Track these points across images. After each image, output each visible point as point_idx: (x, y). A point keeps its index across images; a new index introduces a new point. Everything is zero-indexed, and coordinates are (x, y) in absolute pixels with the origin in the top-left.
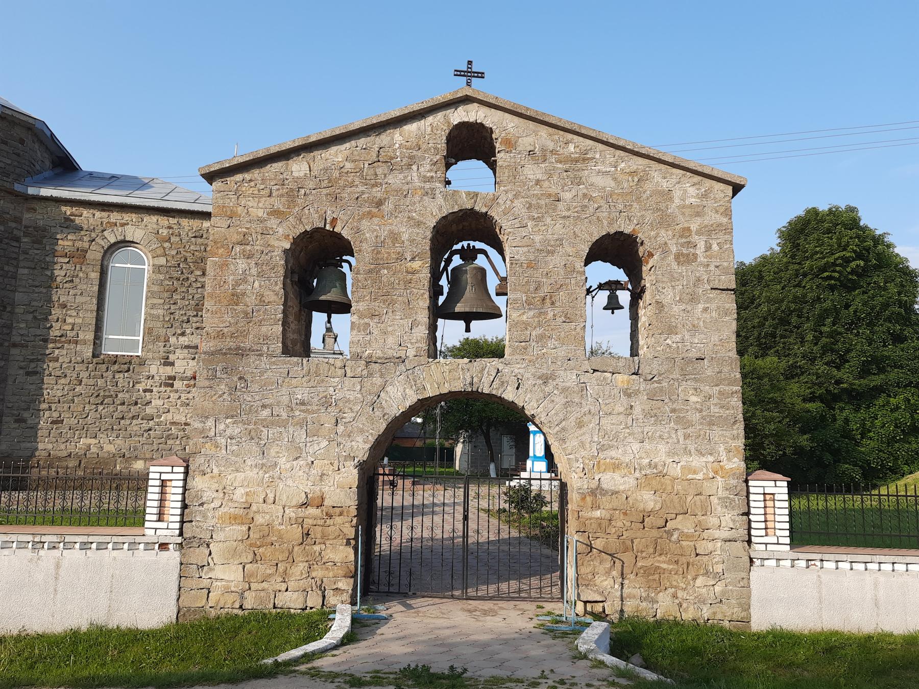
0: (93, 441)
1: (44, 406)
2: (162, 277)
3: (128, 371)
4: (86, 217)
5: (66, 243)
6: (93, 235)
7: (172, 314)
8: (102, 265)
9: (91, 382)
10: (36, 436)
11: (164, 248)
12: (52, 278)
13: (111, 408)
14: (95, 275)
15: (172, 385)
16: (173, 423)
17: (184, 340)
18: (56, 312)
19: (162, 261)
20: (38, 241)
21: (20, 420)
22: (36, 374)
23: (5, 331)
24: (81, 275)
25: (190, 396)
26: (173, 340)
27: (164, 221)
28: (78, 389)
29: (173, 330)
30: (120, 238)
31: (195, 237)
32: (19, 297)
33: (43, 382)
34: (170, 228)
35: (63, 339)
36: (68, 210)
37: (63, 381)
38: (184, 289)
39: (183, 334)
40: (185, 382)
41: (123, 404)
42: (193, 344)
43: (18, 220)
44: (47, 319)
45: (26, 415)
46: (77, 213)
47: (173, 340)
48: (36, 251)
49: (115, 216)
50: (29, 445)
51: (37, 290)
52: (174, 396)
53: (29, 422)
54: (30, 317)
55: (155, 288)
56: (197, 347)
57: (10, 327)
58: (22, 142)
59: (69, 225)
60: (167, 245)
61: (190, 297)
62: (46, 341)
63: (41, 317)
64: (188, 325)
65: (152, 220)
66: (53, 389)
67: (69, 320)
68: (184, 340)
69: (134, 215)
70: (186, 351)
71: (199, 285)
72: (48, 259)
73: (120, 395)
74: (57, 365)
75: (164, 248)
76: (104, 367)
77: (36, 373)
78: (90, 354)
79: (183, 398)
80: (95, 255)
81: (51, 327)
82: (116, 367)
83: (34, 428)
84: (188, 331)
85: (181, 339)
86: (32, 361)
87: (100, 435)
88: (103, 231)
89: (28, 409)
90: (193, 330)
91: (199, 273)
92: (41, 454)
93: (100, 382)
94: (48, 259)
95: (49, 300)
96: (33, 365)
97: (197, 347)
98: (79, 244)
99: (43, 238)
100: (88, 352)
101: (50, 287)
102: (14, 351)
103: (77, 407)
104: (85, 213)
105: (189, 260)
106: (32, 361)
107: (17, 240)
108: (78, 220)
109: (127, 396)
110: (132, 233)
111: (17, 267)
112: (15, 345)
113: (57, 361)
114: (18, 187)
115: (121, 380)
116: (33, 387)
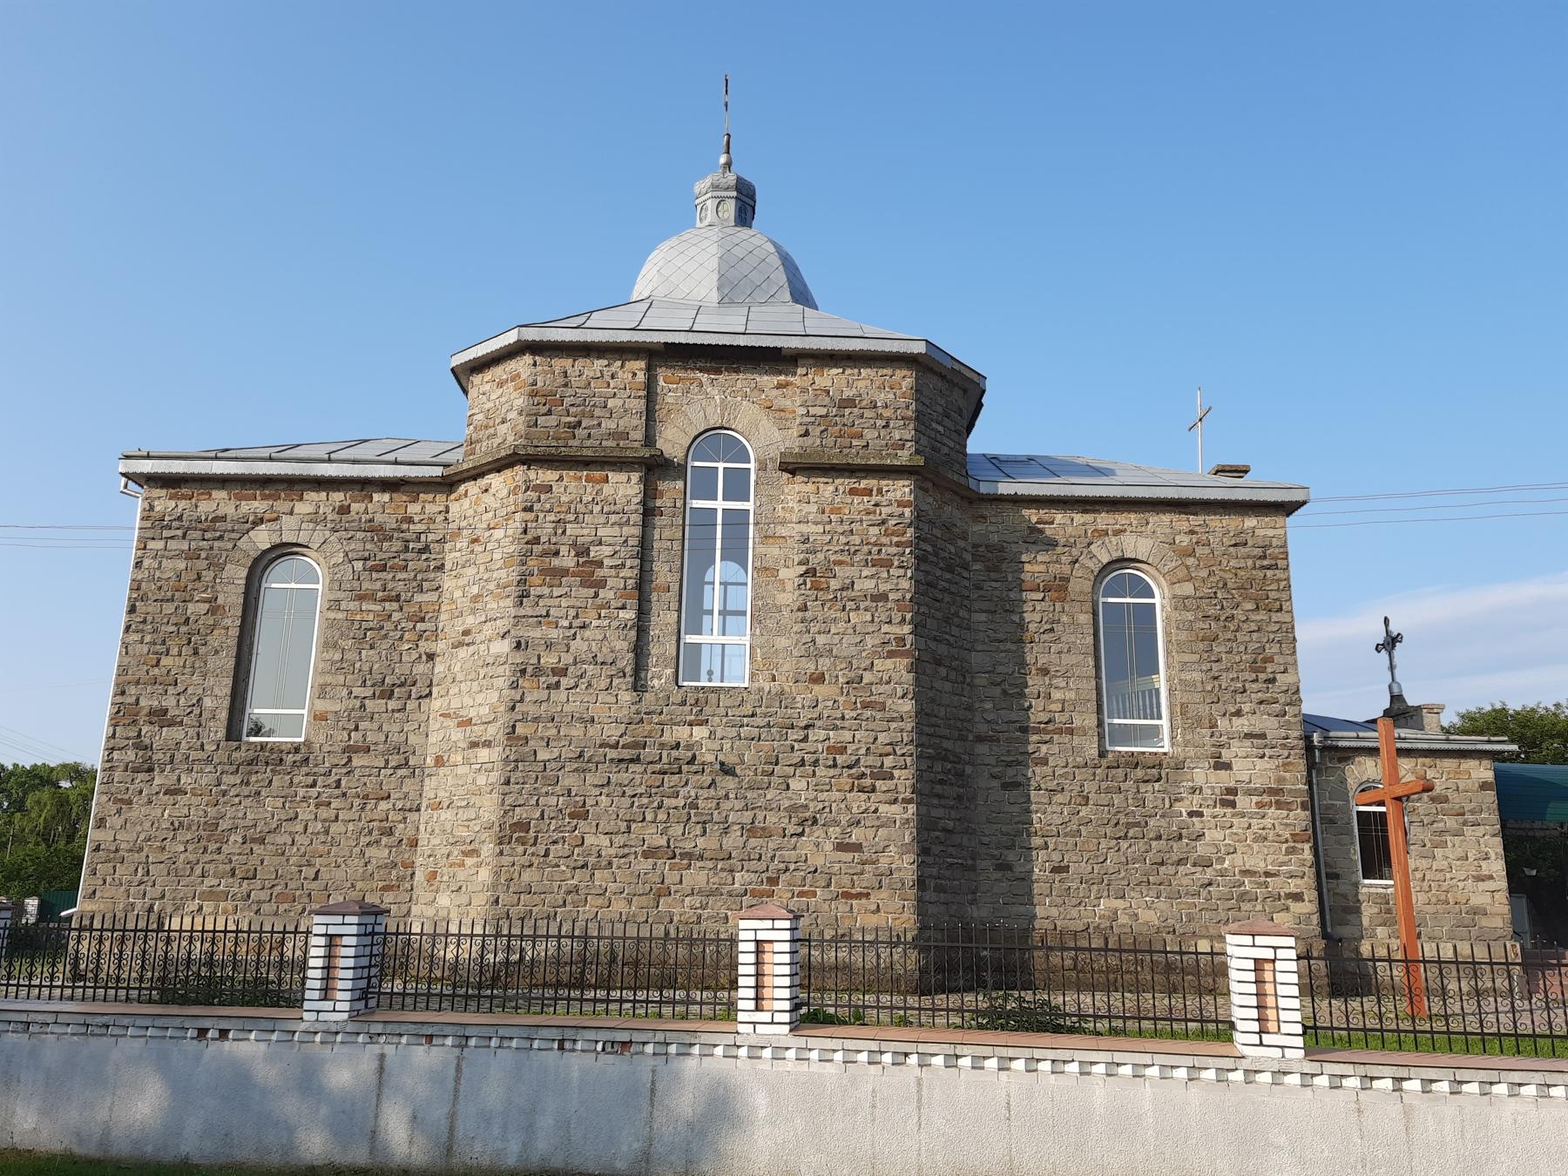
0: (1120, 904)
2: (1190, 616)
3: (1158, 780)
4: (1061, 523)
5: (1036, 567)
6: (1075, 552)
7: (1215, 678)
10: (1030, 894)
11: (1188, 568)
12: (1022, 626)
15: (1233, 804)
16: (1245, 873)
17: (1243, 725)
18: (1034, 683)
19: (1187, 589)
21: (1005, 867)
22: (1018, 785)
24: (1064, 619)
25: (1268, 822)
26: (1222, 724)
27: (1183, 522)
28: (1084, 812)
30: (1116, 555)
31: (1235, 545)
33: (1029, 801)
34: (1192, 532)
35: (1050, 727)
36: (1032, 515)
37: (1059, 798)
38: (1229, 635)
39: (1238, 713)
40: (1255, 799)
41: (1159, 838)
42: (1257, 730)
44: (1022, 695)
45: (1011, 856)
46: (1046, 518)
48: (995, 584)
49: (1104, 520)
50: (1022, 909)
51: (1002, 646)
53: (1017, 869)
54: (997, 691)
56: (1263, 736)
59: (1036, 538)
60: (1191, 561)
61: (1242, 648)
62: (1025, 730)
63: (1014, 692)
64: (1244, 698)
66: (1046, 814)
67: (1056, 695)
68: (1243, 725)
69: (1133, 516)
70: (1248, 743)
71: (1253, 627)
72: (1012, 595)
73: (1152, 822)
74: (1047, 770)
75: (1188, 568)
77: (1017, 785)
78: (1095, 752)
79: (1255, 828)
81: (1030, 707)
82: (1139, 773)
83: (1026, 879)
84: (1246, 708)
86: (1009, 765)
87: (1130, 894)
88: (1089, 544)
89: (1011, 847)
90: (1253, 706)
91: (1250, 606)
93: (1117, 799)
94: (1012, 595)
95: (1023, 664)
96: (1011, 772)
101: (1021, 641)
102: (982, 749)
104: (1059, 517)
105: (1230, 585)
106: (1009, 765)
108: (1049, 531)
109: (1163, 823)
112: (980, 739)
113: (1046, 764)
115: (1149, 796)
116: (1015, 809)
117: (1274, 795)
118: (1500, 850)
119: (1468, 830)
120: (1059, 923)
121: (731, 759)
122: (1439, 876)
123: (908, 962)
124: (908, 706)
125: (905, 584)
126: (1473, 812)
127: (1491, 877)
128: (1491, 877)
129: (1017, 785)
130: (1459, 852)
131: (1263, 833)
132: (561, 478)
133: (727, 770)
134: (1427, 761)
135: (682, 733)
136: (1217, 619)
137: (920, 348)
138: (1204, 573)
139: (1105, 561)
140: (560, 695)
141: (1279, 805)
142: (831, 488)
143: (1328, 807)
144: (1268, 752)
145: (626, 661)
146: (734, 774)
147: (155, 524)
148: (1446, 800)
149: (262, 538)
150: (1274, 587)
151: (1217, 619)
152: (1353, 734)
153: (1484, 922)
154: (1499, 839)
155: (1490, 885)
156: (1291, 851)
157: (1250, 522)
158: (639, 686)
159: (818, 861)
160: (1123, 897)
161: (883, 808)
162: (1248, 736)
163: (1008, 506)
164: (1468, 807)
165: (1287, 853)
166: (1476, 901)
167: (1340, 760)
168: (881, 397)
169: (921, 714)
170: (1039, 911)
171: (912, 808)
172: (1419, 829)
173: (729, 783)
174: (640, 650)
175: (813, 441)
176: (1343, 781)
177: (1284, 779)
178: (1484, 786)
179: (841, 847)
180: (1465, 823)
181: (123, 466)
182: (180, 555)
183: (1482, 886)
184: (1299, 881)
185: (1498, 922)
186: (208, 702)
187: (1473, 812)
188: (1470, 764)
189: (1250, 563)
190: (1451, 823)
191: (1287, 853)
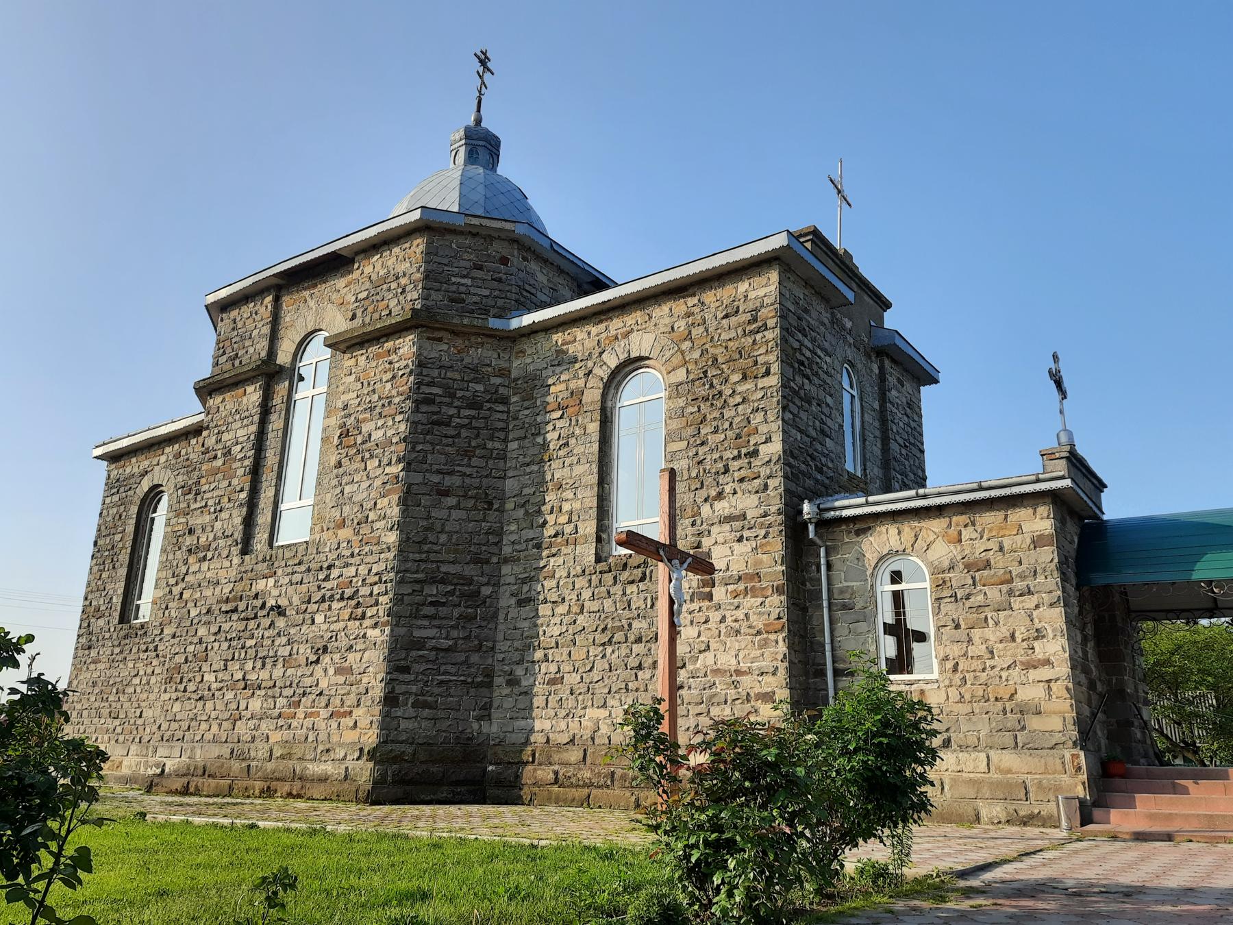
0: (603, 713)
1: (539, 655)
2: (681, 402)
3: (643, 579)
4: (581, 340)
6: (590, 364)
7: (700, 463)
8: (603, 409)
9: (595, 606)
10: (531, 707)
11: (683, 353)
12: (545, 446)
13: (624, 651)
14: (594, 427)
15: (710, 597)
16: (716, 672)
17: (723, 507)
18: (551, 497)
19: (681, 375)
20: (528, 397)
21: (513, 682)
22: (527, 601)
23: (492, 539)
24: (578, 431)
25: (740, 614)
26: (706, 510)
27: (679, 306)
28: (580, 618)
29: (703, 494)
30: (623, 357)
31: (726, 316)
32: (510, 485)
33: (537, 616)
34: (688, 315)
35: (559, 539)
36: (558, 337)
37: (561, 609)
38: (716, 414)
39: (720, 496)
40: (731, 588)
41: (639, 640)
42: (737, 513)
43: (504, 373)
44: (539, 512)
45: (519, 671)
46: (568, 338)
47: (706, 510)
48: (526, 412)
49: (616, 325)
50: (522, 723)
51: (528, 470)
52: (715, 616)
53: (524, 683)
54: (521, 512)
55: (675, 424)
57: (500, 533)
58: (504, 261)
59: (562, 360)
60: (686, 345)
61: (727, 425)
62: (539, 546)
63: (533, 512)
64: (728, 478)
65: (661, 312)
66: (551, 624)
67: (566, 507)
68: (723, 507)
69: (639, 313)
70: (726, 527)
71: (738, 399)
72: (539, 419)
73: (636, 624)
74: (553, 583)
75: (683, 353)
76: (608, 578)
77: (529, 600)
78: (592, 558)
79: (729, 619)
80: (593, 396)
81: (545, 523)
82: (625, 576)
83: (528, 693)
84: (728, 489)
85: (719, 505)
86: (524, 581)
87: (611, 702)
88: (601, 354)
89: (520, 662)
90: (736, 485)
91: (736, 377)
92: (538, 738)
93: (608, 604)
94: (539, 419)
95: (543, 482)
96: (525, 588)
97: (744, 516)
98: (573, 385)
99: (533, 386)
100: (588, 552)
101: (542, 461)
102: (506, 569)
103: (579, 654)
104: (579, 333)
105: (720, 360)
106: (524, 581)
107: (505, 401)
108: (571, 349)
109: (644, 625)
110: (641, 344)
111: (505, 441)
112: (506, 561)
113: (553, 577)
114: (494, 323)
115: (634, 597)
116: (526, 624)
117: (749, 581)
118: (1061, 623)
119: (1016, 602)
120: (551, 736)
121: (283, 602)
122: (976, 664)
123: (364, 771)
124: (392, 538)
125: (402, 427)
126: (1022, 577)
127: (1047, 662)
128: (1047, 662)
129: (529, 600)
130: (1004, 631)
131: (736, 625)
132: (224, 400)
133: (280, 611)
134: (963, 519)
135: (261, 585)
136: (705, 399)
137: (416, 215)
138: (696, 355)
139: (613, 366)
140: (205, 566)
141: (753, 592)
142: (364, 357)
143: (842, 591)
144: (746, 534)
145: (238, 535)
146: (285, 615)
147: (113, 486)
148: (988, 565)
149: (146, 485)
150: (762, 350)
151: (705, 399)
152: (862, 500)
153: (1034, 723)
154: (1059, 611)
155: (1045, 673)
156: (764, 644)
157: (743, 287)
158: (246, 550)
159: (323, 684)
160: (604, 706)
161: (370, 632)
162: (729, 519)
163: (542, 335)
164: (1016, 570)
165: (760, 647)
166: (1025, 694)
167: (858, 533)
168: (402, 267)
169: (404, 546)
170: (538, 725)
171: (387, 630)
172: (952, 606)
173: (281, 623)
174: (249, 523)
175: (358, 322)
176: (861, 557)
177: (761, 562)
178: (1037, 542)
179: (338, 671)
180: (1011, 593)
181: (99, 451)
182: (115, 505)
183: (1034, 674)
184: (769, 679)
185: (1055, 723)
186: (114, 600)
187: (1022, 577)
188: (1021, 515)
189: (740, 330)
190: (994, 594)
191: (760, 647)
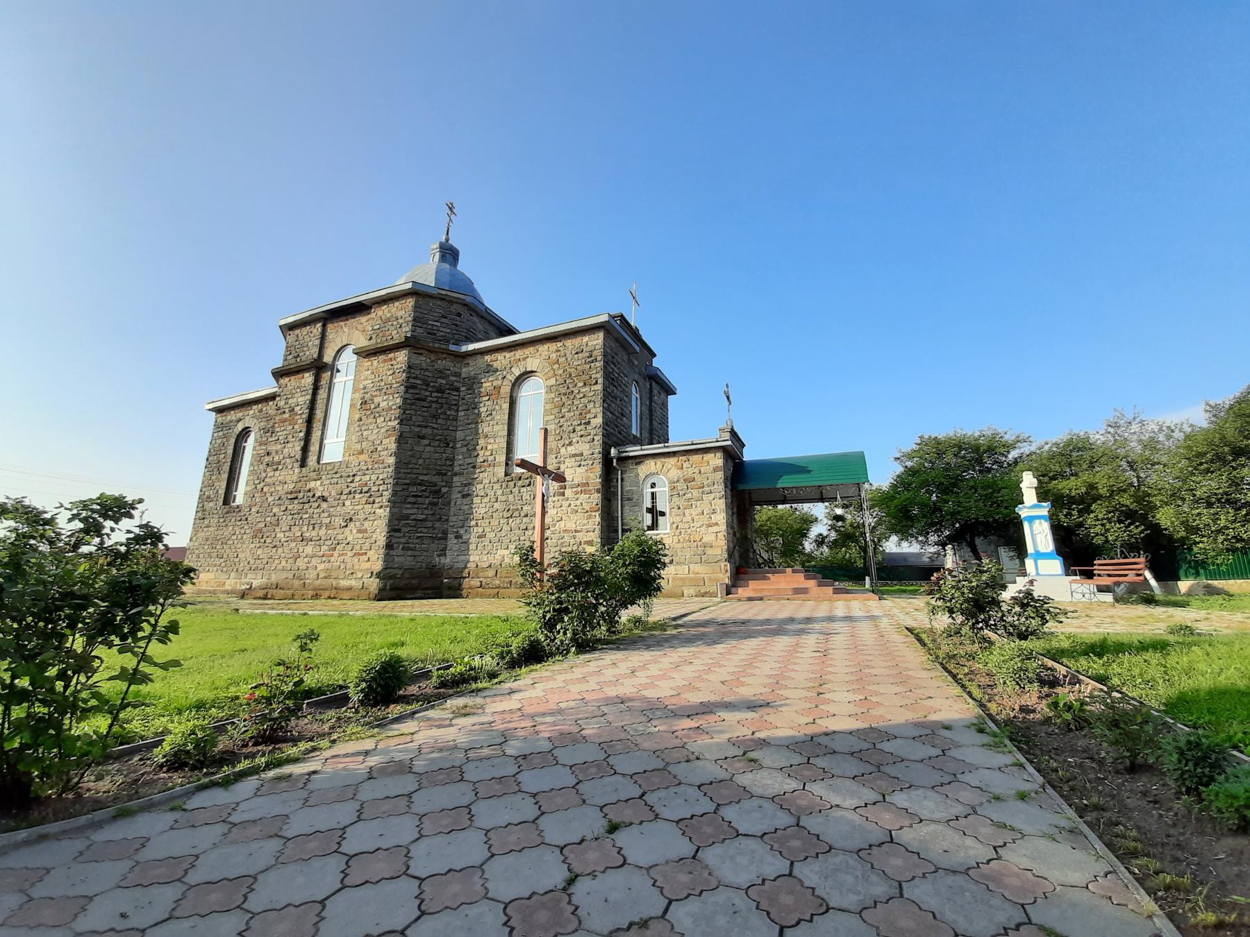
1: (473, 523)
4: (501, 360)
5: (487, 385)
8: (511, 397)
9: (504, 498)
12: (479, 415)
13: (518, 521)
14: (506, 406)
17: (572, 450)
18: (482, 442)
19: (553, 381)
20: (470, 388)
21: (458, 537)
23: (448, 463)
25: (578, 503)
26: (563, 450)
27: (553, 346)
29: (562, 442)
32: (459, 435)
36: (488, 358)
39: (570, 444)
43: (458, 375)
44: (475, 449)
45: (462, 531)
47: (563, 450)
49: (519, 353)
50: (462, 558)
52: (565, 504)
55: (548, 406)
56: (582, 454)
57: (453, 460)
58: (459, 315)
59: (490, 370)
60: (556, 366)
62: (474, 467)
63: (471, 448)
65: (544, 349)
66: (480, 508)
67: (490, 447)
68: (572, 450)
76: (512, 484)
77: (468, 495)
80: (506, 389)
82: (520, 483)
83: (467, 542)
85: (569, 448)
91: (581, 384)
92: (471, 565)
93: (511, 497)
95: (477, 433)
97: (582, 454)
98: (495, 383)
99: (473, 384)
100: (501, 471)
102: (456, 479)
103: (494, 522)
104: (500, 356)
107: (457, 390)
108: (495, 364)
110: (532, 364)
111: (457, 411)
112: (456, 474)
114: (452, 347)
117: (583, 486)
121: (326, 494)
122: (686, 526)
123: (374, 584)
124: (392, 460)
125: (398, 400)
129: (468, 495)
133: (324, 499)
135: (312, 484)
137: (409, 286)
138: (561, 372)
140: (277, 473)
141: (585, 492)
145: (299, 456)
147: (219, 427)
148: (694, 480)
149: (240, 427)
153: (709, 551)
154: (723, 500)
155: (715, 529)
157: (586, 339)
159: (350, 539)
162: (574, 455)
169: (399, 465)
170: (472, 559)
173: (324, 505)
174: (305, 450)
175: (373, 342)
176: (637, 475)
178: (716, 470)
179: (359, 531)
181: (211, 406)
190: (696, 493)
